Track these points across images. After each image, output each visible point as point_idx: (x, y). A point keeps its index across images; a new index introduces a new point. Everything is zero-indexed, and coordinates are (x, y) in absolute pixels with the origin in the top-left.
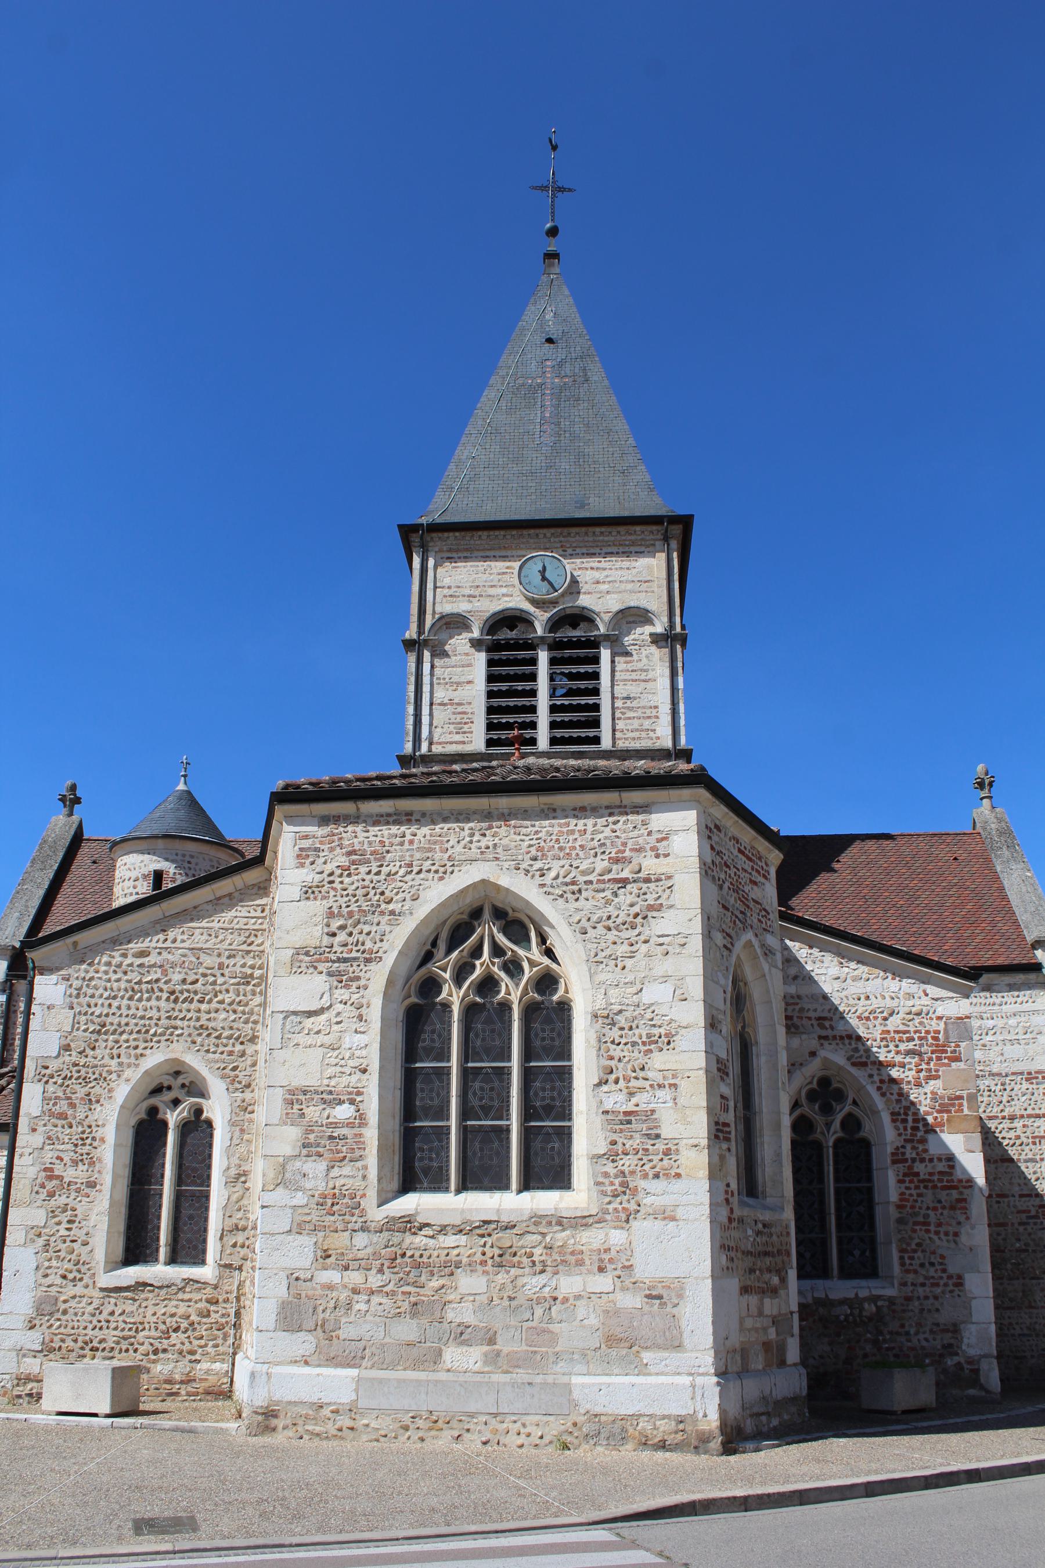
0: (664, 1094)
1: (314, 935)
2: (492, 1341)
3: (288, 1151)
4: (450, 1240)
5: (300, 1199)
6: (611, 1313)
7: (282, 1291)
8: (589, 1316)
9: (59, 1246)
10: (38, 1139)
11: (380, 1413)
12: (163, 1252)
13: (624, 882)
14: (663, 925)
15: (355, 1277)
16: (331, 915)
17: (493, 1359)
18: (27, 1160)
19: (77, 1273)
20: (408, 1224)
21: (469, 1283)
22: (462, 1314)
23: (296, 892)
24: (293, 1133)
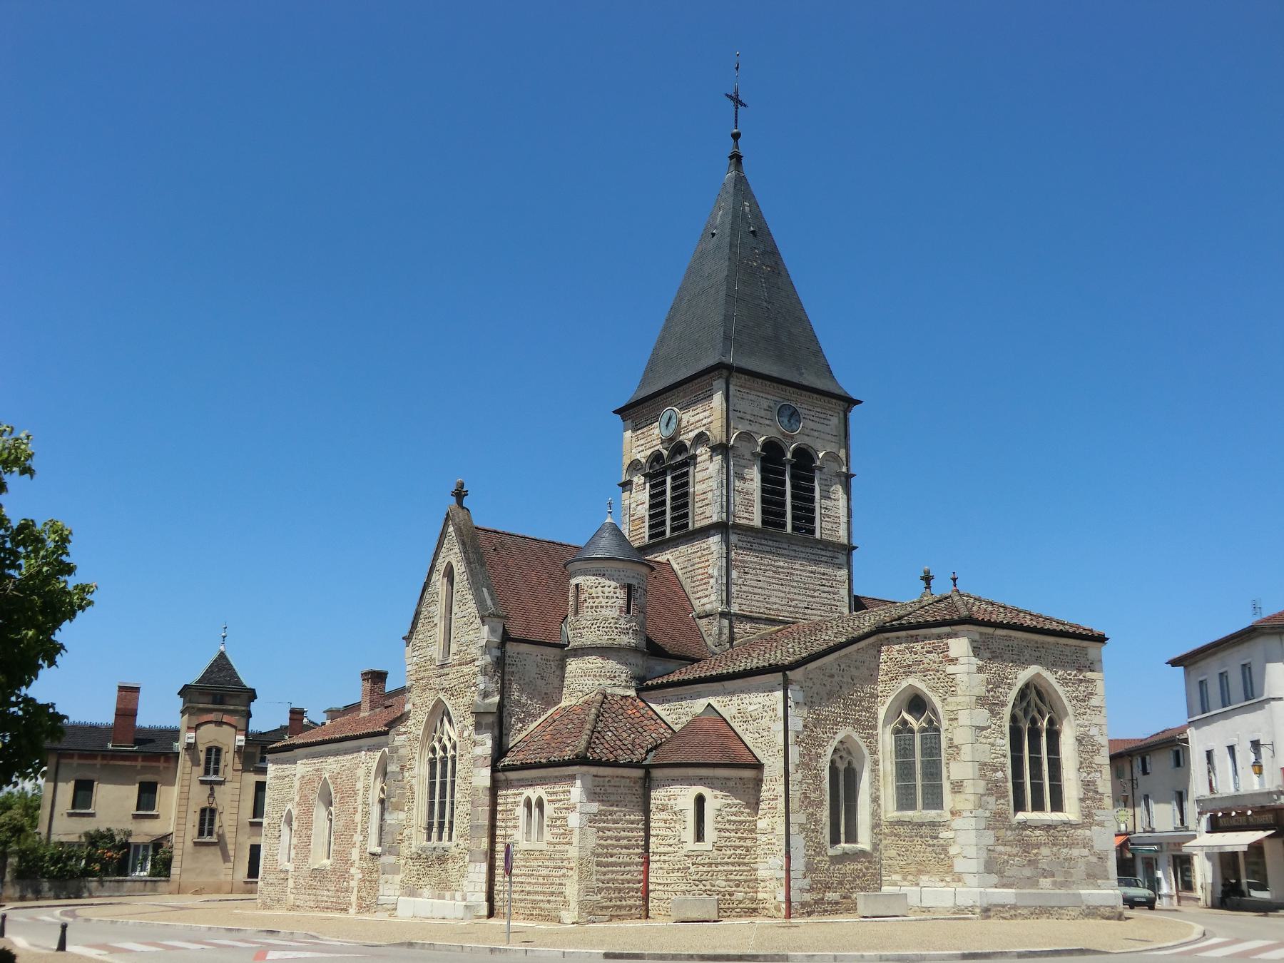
0: (1098, 774)
1: (981, 691)
2: (1053, 876)
3: (982, 791)
4: (1037, 833)
5: (988, 814)
6: (1088, 863)
7: (985, 855)
8: (1082, 867)
9: (810, 833)
10: (799, 776)
11: (1025, 907)
12: (843, 837)
13: (1081, 681)
14: (1095, 701)
15: (1008, 849)
16: (988, 683)
17: (1054, 883)
18: (796, 788)
19: (819, 850)
20: (1024, 825)
21: (1045, 851)
22: (1043, 864)
23: (974, 669)
24: (983, 783)
